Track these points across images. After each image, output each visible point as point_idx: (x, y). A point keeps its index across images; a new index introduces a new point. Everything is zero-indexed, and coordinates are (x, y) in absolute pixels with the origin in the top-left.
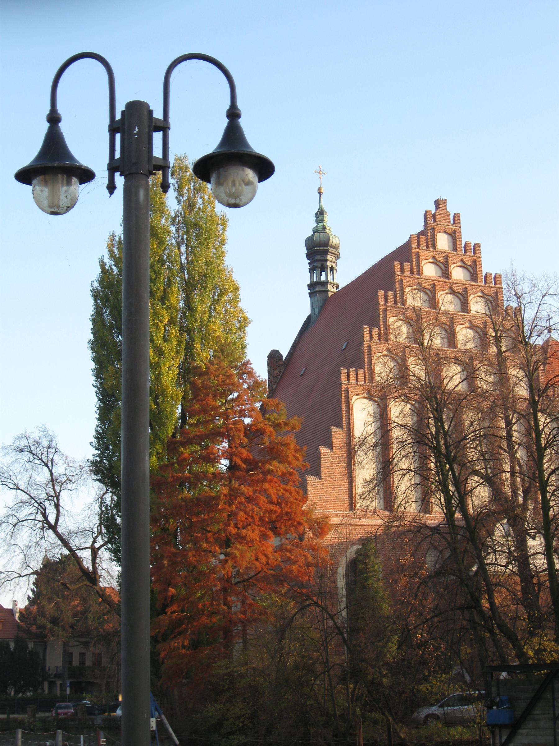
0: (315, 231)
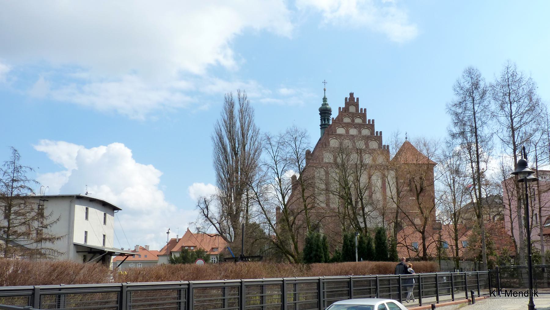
0: (323, 105)
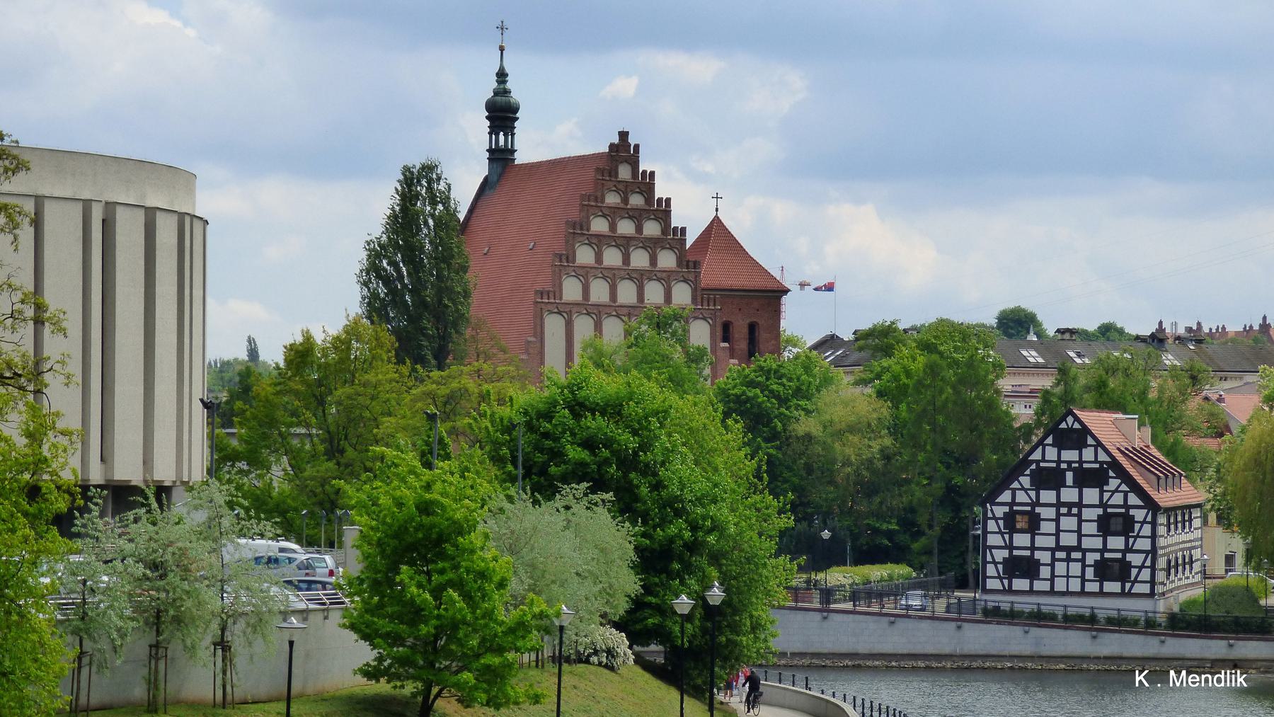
0: (496, 93)
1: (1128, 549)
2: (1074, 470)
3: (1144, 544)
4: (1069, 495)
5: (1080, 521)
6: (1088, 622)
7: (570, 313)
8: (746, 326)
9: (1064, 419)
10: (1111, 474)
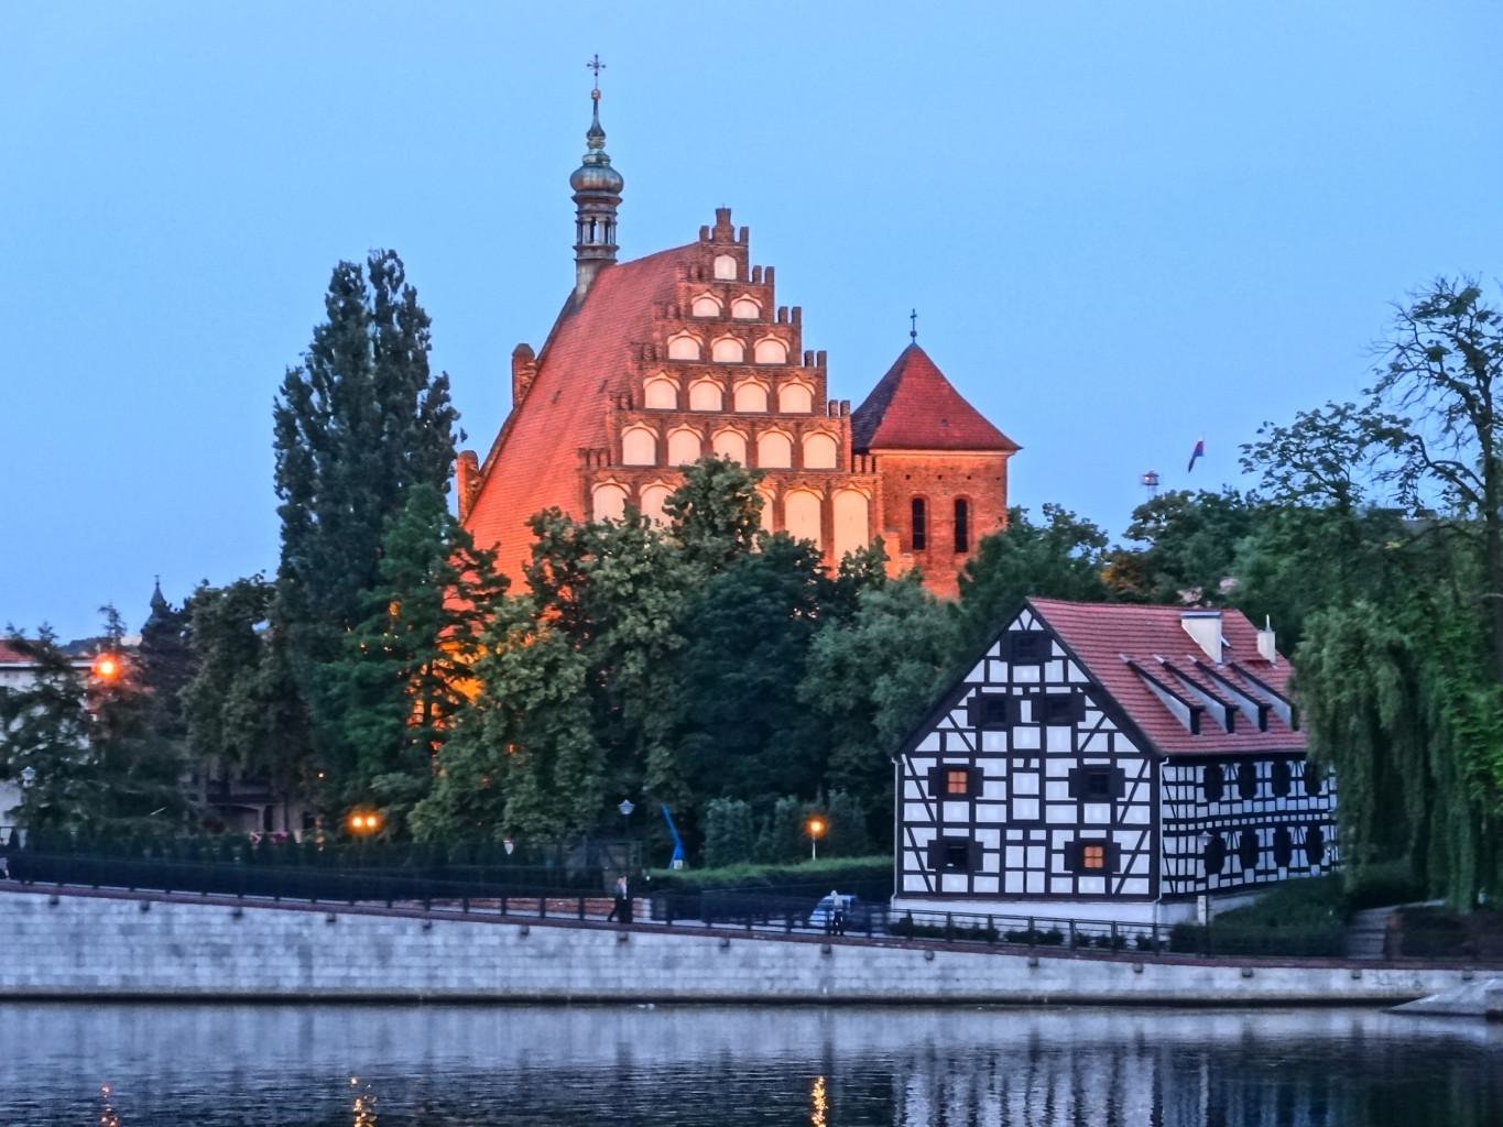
0: (587, 165)
1: (1116, 824)
2: (1032, 697)
3: (1140, 815)
4: (1026, 738)
5: (1043, 780)
6: (1037, 943)
7: (635, 486)
8: (952, 502)
9: (1017, 616)
10: (1089, 702)
